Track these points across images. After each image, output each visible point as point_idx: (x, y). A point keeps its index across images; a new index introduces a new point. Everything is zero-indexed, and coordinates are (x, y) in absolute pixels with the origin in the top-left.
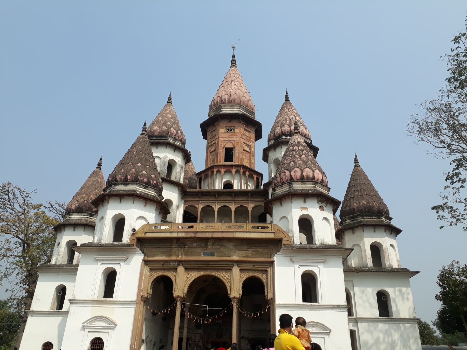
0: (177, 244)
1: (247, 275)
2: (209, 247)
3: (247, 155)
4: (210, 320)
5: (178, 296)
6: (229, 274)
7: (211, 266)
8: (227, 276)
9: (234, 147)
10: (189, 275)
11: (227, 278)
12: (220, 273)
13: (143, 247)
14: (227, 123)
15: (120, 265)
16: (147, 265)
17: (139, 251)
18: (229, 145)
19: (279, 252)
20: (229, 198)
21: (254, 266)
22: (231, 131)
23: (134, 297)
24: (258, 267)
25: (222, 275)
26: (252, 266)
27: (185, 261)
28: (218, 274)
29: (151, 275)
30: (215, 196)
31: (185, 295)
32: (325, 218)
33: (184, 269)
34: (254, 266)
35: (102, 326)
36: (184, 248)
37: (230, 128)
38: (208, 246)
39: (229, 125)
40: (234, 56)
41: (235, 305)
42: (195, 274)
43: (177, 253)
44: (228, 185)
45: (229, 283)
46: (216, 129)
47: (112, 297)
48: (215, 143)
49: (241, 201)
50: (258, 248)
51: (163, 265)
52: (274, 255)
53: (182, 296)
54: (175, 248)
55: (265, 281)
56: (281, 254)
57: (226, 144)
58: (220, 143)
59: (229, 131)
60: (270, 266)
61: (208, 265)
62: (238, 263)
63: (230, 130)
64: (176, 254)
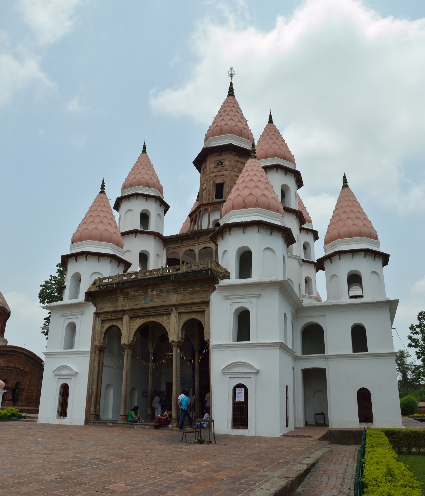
0: (121, 294)
2: (149, 293)
4: (153, 365)
5: (124, 344)
6: (169, 319)
7: (151, 312)
8: (168, 321)
9: (225, 182)
10: (134, 324)
11: (167, 323)
12: (161, 319)
13: (95, 300)
14: (216, 156)
15: (78, 319)
16: (99, 317)
17: (91, 305)
18: (219, 181)
19: (215, 290)
21: (191, 307)
22: (221, 165)
23: (88, 348)
24: (195, 309)
26: (190, 308)
27: (128, 310)
28: (159, 320)
29: (103, 326)
31: (131, 342)
33: (129, 318)
34: (191, 307)
35: (66, 374)
36: (127, 297)
37: (220, 162)
38: (148, 293)
39: (219, 158)
42: (139, 322)
43: (122, 303)
45: (169, 327)
46: (207, 166)
48: (206, 180)
50: (195, 289)
51: (111, 315)
52: (210, 294)
53: (127, 343)
54: (120, 298)
55: (203, 323)
56: (218, 291)
57: (215, 181)
58: (208, 179)
59: (219, 165)
60: (207, 306)
61: (149, 311)
62: (177, 306)
64: (121, 304)
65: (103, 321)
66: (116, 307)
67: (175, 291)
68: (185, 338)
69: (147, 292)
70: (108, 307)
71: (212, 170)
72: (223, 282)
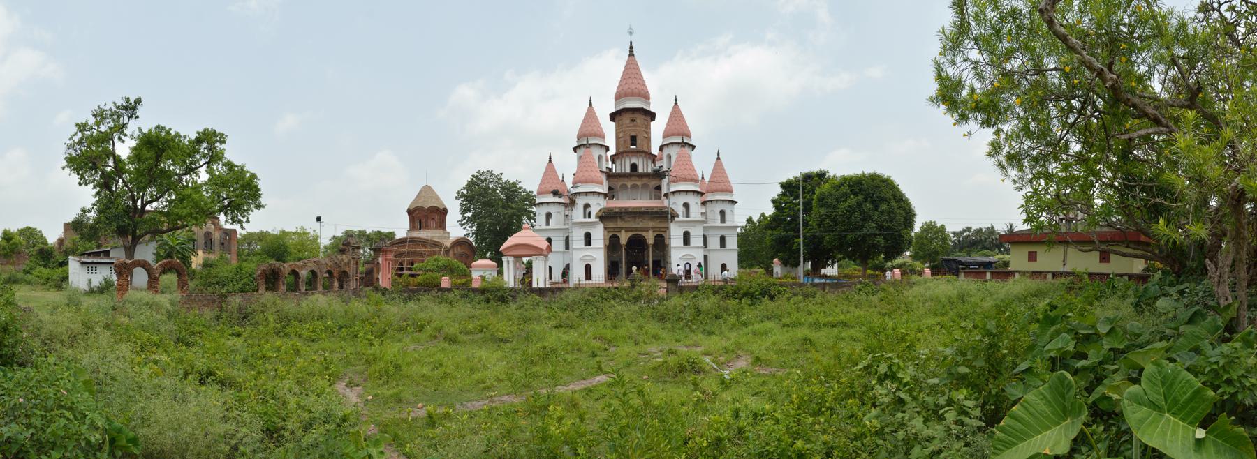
1: (656, 234)
3: (646, 140)
18: (633, 134)
20: (637, 179)
23: (603, 246)
24: (662, 230)
25: (644, 234)
27: (626, 228)
30: (628, 177)
32: (697, 203)
39: (633, 116)
40: (631, 43)
41: (650, 249)
44: (634, 167)
47: (590, 245)
49: (645, 180)
54: (619, 220)
63: (633, 121)
65: (608, 232)
66: (617, 225)
67: (651, 220)
68: (655, 243)
69: (635, 219)
70: (611, 225)
71: (629, 125)
72: (676, 219)
